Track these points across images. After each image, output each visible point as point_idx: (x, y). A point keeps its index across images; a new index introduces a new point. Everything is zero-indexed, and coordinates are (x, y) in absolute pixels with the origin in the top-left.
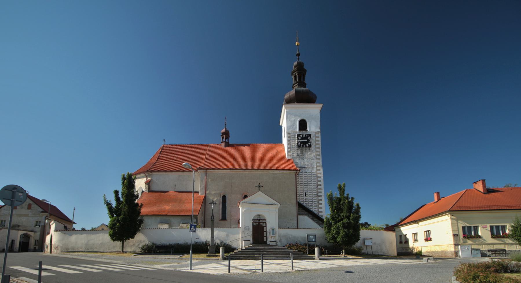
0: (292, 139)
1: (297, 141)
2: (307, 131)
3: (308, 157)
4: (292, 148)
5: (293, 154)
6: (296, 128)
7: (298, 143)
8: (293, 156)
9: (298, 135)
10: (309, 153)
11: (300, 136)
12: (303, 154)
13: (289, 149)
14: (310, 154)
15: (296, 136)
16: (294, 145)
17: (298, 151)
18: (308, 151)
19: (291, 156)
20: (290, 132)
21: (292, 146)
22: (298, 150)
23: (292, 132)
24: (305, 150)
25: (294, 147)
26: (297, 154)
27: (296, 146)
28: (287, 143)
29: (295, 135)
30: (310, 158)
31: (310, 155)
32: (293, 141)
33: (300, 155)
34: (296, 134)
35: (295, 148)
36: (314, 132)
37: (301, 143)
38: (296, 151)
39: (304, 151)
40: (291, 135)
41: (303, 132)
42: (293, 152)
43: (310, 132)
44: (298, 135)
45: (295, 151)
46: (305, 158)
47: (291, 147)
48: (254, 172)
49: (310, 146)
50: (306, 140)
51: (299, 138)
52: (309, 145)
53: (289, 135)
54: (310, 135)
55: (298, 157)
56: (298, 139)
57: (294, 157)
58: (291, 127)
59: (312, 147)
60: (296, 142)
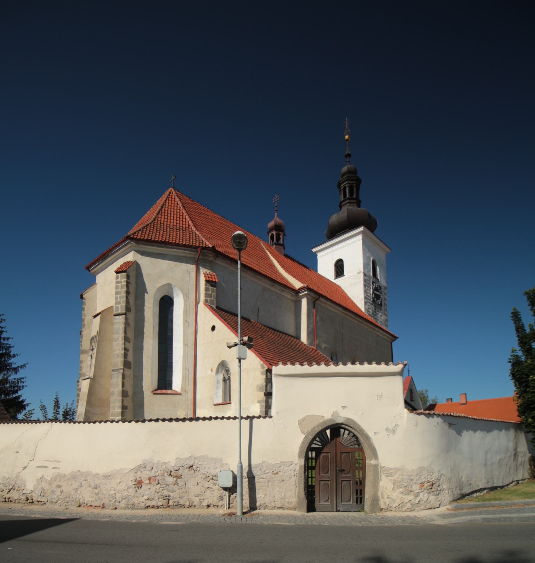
0: (367, 284)
1: (371, 290)
2: (378, 280)
3: (380, 320)
4: (368, 299)
5: (369, 308)
6: (369, 271)
7: (372, 295)
8: (369, 312)
9: (372, 281)
10: (380, 314)
11: (374, 285)
12: (375, 312)
13: (366, 300)
14: (381, 316)
15: (370, 282)
16: (369, 295)
17: (372, 306)
18: (380, 311)
19: (367, 310)
20: (366, 274)
21: (368, 296)
22: (372, 304)
23: (368, 275)
24: (378, 308)
25: (369, 298)
26: (372, 310)
27: (371, 298)
28: (364, 288)
29: (369, 281)
30: (381, 322)
31: (381, 317)
32: (369, 289)
33: (374, 313)
34: (370, 279)
35: (370, 300)
36: (384, 286)
37: (376, 295)
38: (371, 305)
39: (377, 309)
40: (367, 278)
41: (375, 280)
42: (368, 305)
43: (380, 284)
44: (373, 282)
45: (370, 306)
46: (378, 320)
47: (367, 297)
48: (362, 323)
49: (381, 305)
50: (379, 294)
51: (374, 288)
52: (380, 301)
53: (365, 277)
54: (380, 287)
55: (373, 315)
56: (372, 289)
57: (370, 314)
58: (367, 267)
59: (382, 307)
60: (370, 291)
